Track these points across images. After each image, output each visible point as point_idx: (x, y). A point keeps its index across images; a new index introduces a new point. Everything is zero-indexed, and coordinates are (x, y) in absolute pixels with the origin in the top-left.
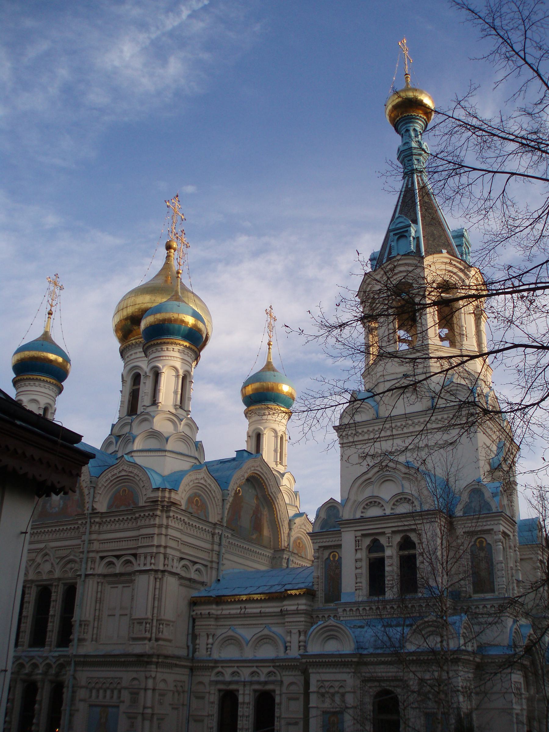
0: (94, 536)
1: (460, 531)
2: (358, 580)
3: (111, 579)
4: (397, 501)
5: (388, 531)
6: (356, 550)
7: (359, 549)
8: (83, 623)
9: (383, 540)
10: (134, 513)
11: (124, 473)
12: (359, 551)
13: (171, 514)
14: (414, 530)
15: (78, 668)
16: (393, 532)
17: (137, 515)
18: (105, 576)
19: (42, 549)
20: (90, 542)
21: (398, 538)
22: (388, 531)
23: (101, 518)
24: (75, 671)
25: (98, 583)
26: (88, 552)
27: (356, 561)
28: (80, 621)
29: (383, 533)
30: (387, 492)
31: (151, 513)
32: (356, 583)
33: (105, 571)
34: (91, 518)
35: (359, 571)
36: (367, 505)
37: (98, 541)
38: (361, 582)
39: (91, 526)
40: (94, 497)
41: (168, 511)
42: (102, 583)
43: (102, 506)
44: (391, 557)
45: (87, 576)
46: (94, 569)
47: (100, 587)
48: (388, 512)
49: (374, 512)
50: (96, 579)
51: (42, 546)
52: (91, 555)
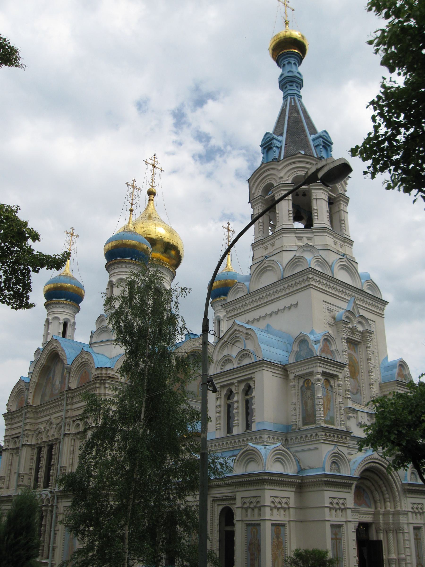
0: (69, 407)
1: (292, 376)
2: (218, 422)
3: (78, 436)
4: (241, 357)
5: (235, 381)
6: (217, 399)
7: (219, 398)
8: (62, 468)
9: (234, 389)
10: (86, 388)
11: (83, 360)
12: (219, 399)
13: (107, 385)
14: (251, 379)
15: (60, 501)
16: (240, 382)
17: (88, 388)
18: (76, 434)
19: (48, 421)
20: (67, 411)
21: (242, 387)
22: (235, 381)
23: (72, 393)
24: (58, 502)
25: (72, 439)
26: (66, 418)
27: (217, 407)
28: (61, 467)
29: (232, 384)
30: (234, 352)
31: (94, 386)
32: (217, 424)
33: (76, 431)
34: (67, 394)
35: (218, 415)
36: (224, 362)
37: (72, 410)
38: (220, 424)
39: (67, 400)
40: (69, 379)
41: (104, 383)
42: (74, 439)
43: (73, 386)
44: (237, 402)
45: (65, 435)
46: (69, 430)
47: (73, 442)
48: (235, 366)
49: (229, 367)
50: (71, 437)
51: (48, 418)
52: (68, 420)
